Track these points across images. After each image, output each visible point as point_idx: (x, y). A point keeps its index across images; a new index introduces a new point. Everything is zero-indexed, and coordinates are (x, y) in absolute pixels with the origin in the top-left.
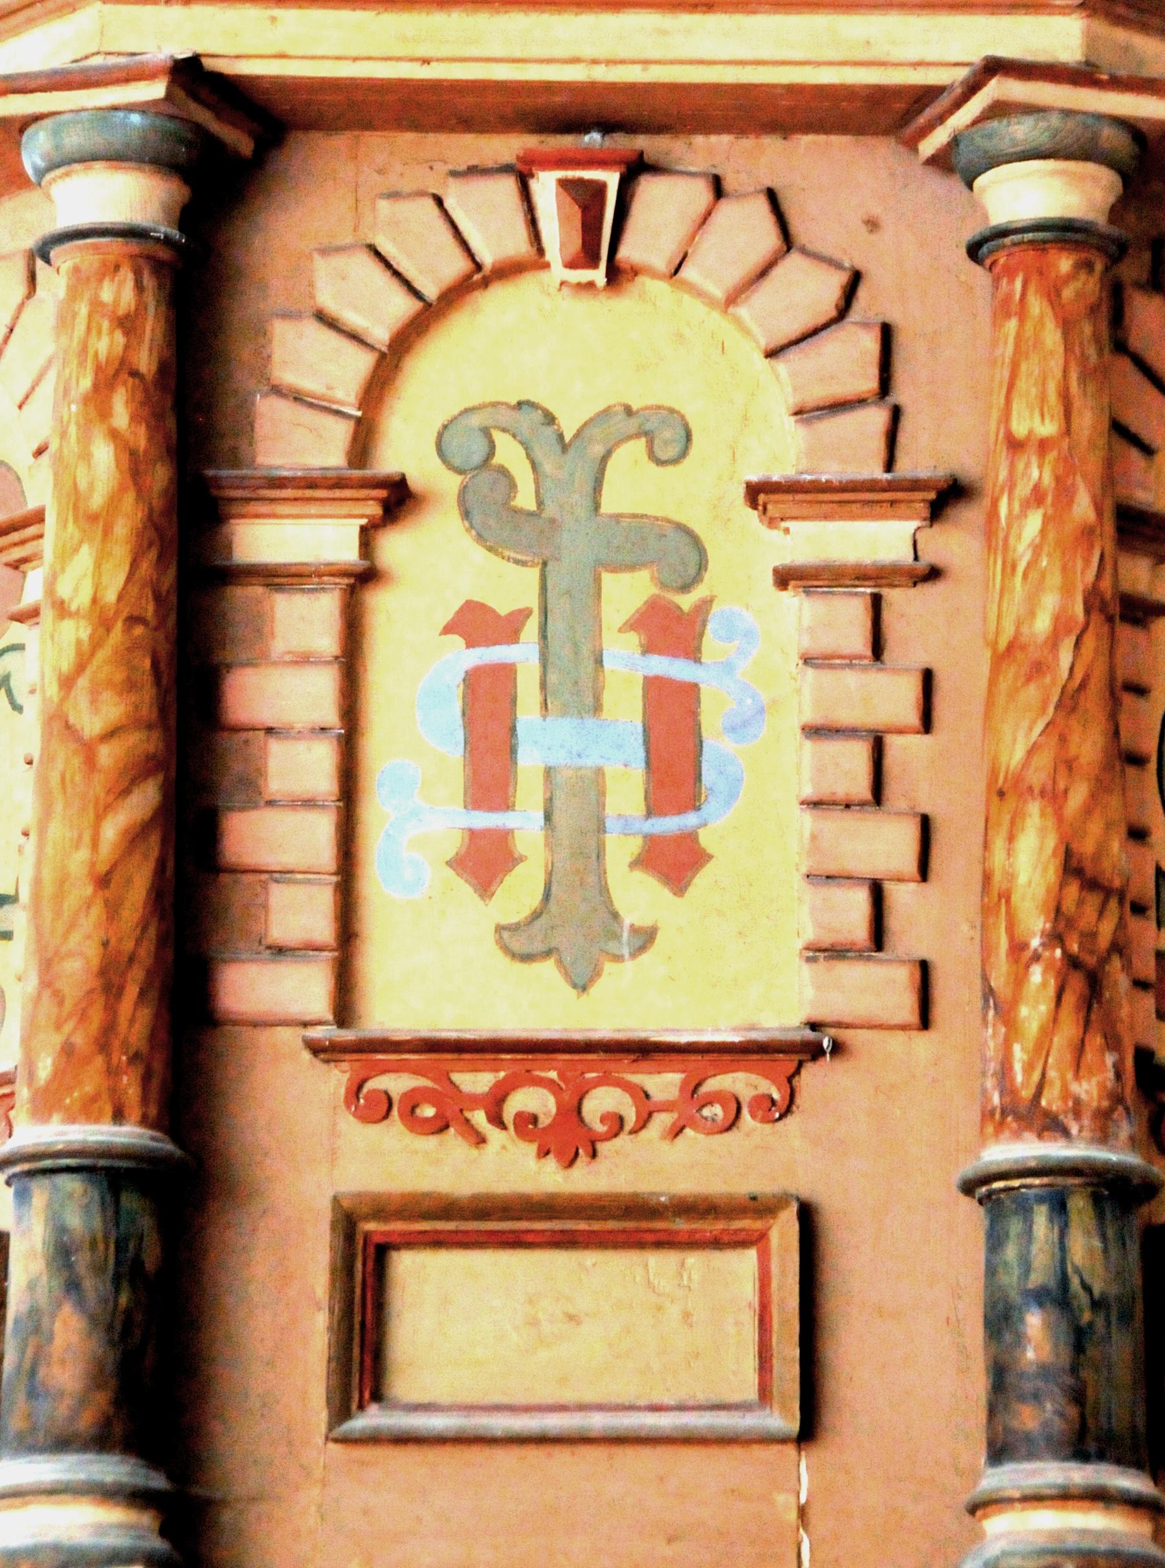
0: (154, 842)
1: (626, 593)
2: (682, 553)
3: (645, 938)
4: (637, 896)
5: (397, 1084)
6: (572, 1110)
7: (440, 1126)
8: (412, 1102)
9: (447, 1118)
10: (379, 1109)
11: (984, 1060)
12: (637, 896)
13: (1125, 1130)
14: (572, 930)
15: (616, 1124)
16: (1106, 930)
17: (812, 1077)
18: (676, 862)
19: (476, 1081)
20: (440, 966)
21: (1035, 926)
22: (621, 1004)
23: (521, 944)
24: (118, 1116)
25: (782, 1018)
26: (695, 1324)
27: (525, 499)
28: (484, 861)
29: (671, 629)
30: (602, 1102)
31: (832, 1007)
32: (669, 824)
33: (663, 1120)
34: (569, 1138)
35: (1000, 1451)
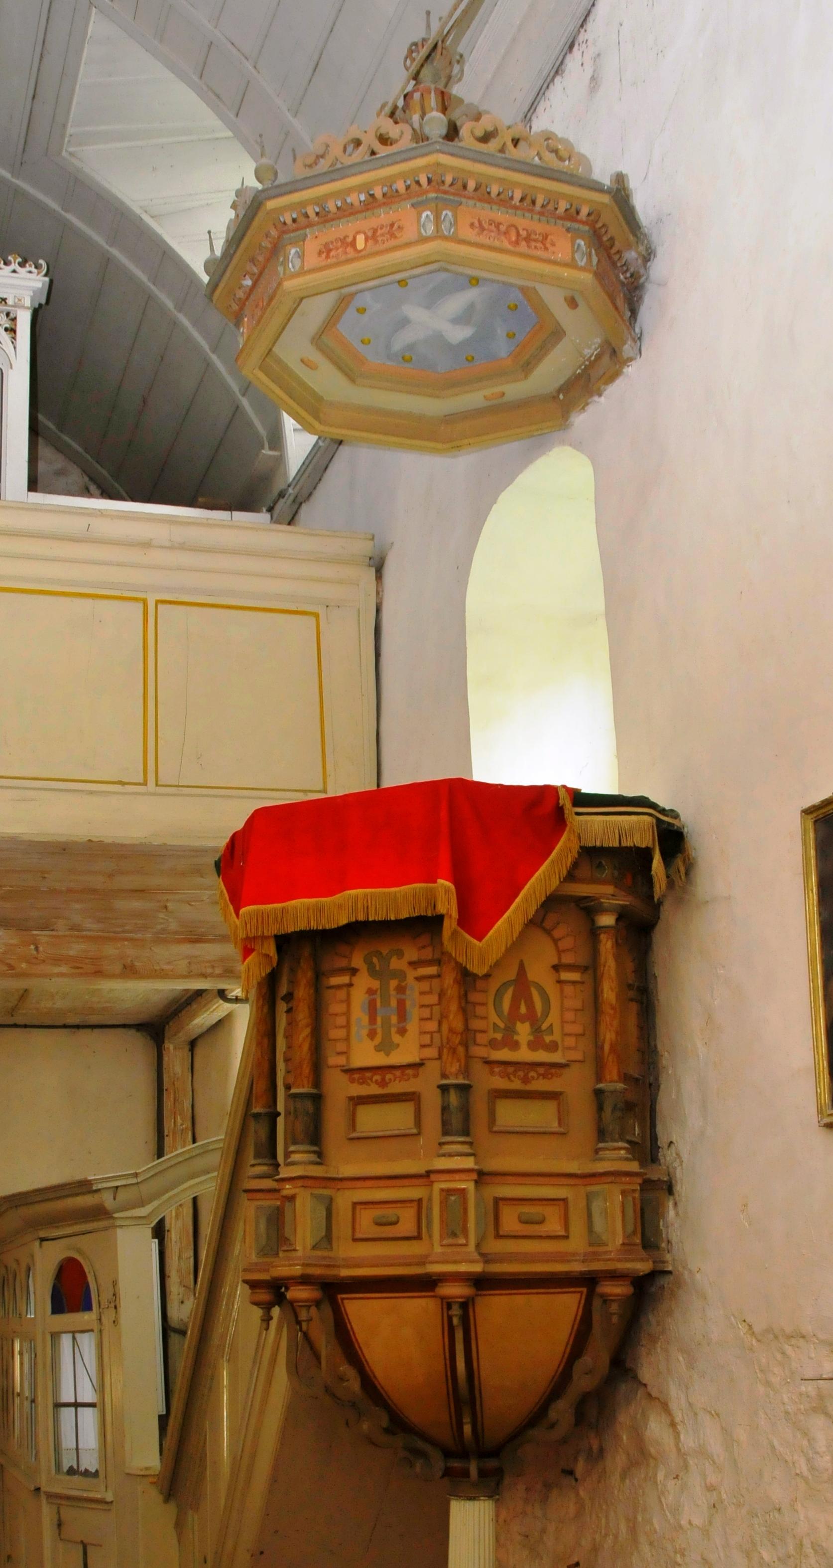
0: (309, 1039)
1: (394, 983)
2: (401, 975)
3: (398, 1045)
4: (396, 1038)
5: (356, 1076)
6: (383, 1079)
7: (363, 1083)
8: (359, 1079)
9: (363, 1082)
10: (352, 1081)
11: (180, 1114)
12: (396, 1038)
13: (461, 1077)
14: (386, 1046)
15: (390, 1079)
16: (457, 1042)
17: (421, 1070)
18: (402, 1032)
19: (368, 1075)
20: (365, 1055)
21: (445, 1041)
22: (396, 1058)
23: (378, 1049)
24: (303, 1087)
25: (417, 1060)
26: (397, 1118)
27: (377, 968)
28: (372, 1035)
29: (401, 989)
30: (388, 1076)
31: (423, 1056)
32: (401, 1025)
33: (398, 1080)
34: (383, 1083)
35: (445, 1133)
